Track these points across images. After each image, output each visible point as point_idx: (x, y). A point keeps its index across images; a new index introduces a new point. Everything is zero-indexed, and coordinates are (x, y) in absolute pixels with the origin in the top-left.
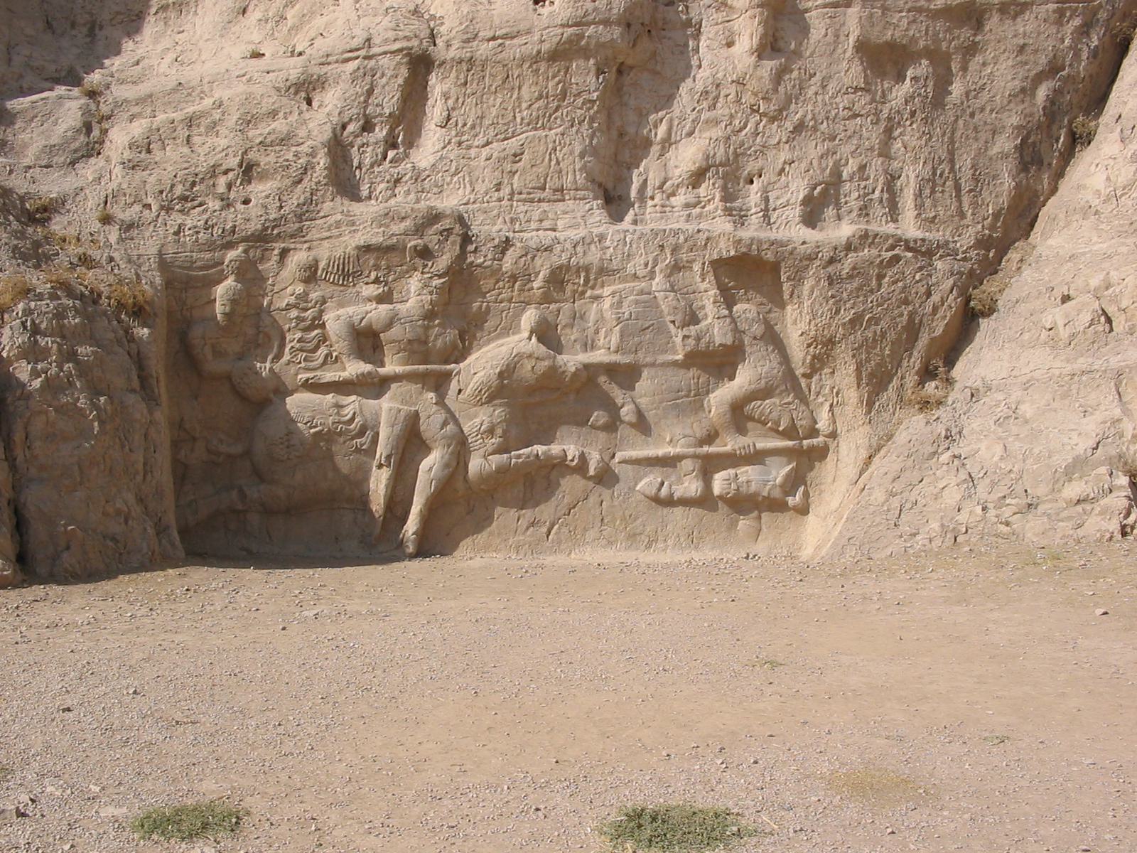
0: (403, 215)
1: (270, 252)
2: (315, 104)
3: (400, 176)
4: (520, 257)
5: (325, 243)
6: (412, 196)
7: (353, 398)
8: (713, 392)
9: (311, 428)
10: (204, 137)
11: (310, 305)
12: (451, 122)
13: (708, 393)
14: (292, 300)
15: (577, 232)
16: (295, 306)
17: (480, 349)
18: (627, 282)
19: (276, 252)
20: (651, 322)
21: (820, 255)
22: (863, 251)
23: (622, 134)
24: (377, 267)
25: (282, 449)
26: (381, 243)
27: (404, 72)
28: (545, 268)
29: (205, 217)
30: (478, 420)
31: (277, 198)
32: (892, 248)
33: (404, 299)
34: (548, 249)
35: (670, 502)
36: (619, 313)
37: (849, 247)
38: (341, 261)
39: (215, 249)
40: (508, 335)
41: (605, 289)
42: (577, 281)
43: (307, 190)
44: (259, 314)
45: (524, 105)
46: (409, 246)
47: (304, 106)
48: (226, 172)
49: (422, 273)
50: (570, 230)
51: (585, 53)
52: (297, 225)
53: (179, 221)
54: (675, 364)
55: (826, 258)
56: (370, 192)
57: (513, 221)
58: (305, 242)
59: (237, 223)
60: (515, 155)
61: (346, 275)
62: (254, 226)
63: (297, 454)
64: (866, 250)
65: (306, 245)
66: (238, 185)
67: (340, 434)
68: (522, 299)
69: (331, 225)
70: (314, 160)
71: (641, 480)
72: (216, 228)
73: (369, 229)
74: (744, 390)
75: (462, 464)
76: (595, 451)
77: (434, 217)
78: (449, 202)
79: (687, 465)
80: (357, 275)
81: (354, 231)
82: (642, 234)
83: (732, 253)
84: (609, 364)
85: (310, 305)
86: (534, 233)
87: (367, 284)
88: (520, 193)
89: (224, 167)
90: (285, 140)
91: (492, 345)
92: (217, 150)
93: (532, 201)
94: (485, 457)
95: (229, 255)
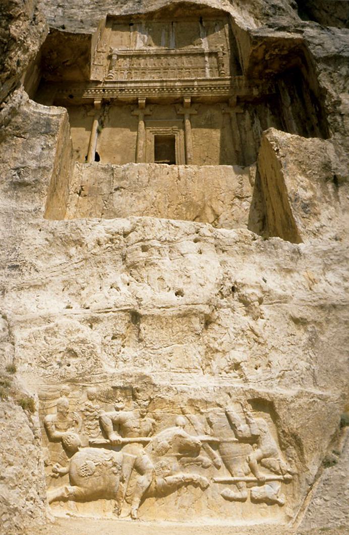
2: (93, 328)
5: (99, 384)
13: (248, 454)
14: (87, 408)
16: (87, 410)
27: (128, 318)
30: (161, 462)
32: (312, 397)
34: (185, 392)
35: (231, 500)
47: (90, 329)
48: (60, 352)
54: (236, 442)
55: (290, 401)
57: (172, 380)
60: (170, 353)
61: (108, 398)
62: (73, 376)
65: (92, 385)
67: (106, 466)
77: (142, 377)
78: (147, 371)
79: (241, 484)
81: (111, 380)
90: (83, 341)
94: (163, 478)
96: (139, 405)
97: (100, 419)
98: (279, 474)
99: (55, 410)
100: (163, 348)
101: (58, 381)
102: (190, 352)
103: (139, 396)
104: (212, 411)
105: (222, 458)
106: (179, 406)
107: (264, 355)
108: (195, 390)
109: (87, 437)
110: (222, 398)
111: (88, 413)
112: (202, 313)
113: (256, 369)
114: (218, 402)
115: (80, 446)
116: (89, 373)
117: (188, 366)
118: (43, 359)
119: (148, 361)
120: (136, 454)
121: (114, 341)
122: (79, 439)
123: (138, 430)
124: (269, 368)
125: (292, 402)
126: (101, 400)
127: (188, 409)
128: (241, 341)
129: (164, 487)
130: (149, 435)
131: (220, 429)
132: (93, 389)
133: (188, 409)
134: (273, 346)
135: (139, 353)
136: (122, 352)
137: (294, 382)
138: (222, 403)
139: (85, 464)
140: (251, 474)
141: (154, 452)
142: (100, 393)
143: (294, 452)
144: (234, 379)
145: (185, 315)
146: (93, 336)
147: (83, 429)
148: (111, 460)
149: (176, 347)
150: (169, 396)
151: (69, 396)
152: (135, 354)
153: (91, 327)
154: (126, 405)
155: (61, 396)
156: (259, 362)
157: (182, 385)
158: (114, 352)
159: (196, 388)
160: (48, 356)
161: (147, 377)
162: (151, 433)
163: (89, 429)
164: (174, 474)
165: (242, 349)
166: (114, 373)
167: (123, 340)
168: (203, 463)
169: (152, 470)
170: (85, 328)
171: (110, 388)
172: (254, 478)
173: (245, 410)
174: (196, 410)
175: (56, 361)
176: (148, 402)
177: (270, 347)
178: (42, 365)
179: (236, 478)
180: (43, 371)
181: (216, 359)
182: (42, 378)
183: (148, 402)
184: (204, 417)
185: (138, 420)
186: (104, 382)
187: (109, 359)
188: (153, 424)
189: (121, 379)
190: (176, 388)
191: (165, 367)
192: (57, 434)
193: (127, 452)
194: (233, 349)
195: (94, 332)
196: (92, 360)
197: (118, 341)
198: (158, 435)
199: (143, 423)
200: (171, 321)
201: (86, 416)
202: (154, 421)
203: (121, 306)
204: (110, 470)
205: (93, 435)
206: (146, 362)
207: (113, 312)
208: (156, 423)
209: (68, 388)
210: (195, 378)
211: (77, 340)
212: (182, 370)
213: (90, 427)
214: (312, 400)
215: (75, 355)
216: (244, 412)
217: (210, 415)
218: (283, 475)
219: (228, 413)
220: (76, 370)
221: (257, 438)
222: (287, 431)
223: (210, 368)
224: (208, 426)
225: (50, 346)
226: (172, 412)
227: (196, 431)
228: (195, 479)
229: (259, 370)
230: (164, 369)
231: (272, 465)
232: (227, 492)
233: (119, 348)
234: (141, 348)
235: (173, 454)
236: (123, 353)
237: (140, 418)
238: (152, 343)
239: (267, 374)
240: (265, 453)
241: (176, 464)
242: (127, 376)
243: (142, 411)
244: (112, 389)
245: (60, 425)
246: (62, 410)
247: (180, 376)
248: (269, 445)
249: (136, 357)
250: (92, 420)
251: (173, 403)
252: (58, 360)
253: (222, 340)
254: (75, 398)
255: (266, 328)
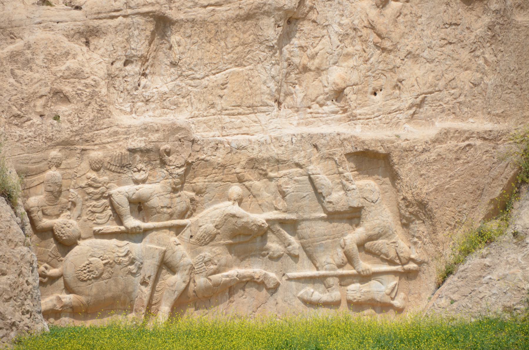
0: (156, 128)
1: (74, 151)
2: (92, 47)
3: (150, 98)
4: (227, 154)
5: (108, 146)
6: (158, 112)
7: (126, 242)
8: (345, 236)
9: (102, 260)
10: (22, 71)
11: (100, 185)
12: (182, 61)
13: (343, 235)
14: (90, 182)
15: (262, 135)
16: (90, 186)
17: (202, 211)
18: (292, 168)
19: (79, 151)
20: (307, 193)
21: (416, 147)
22: (446, 143)
23: (290, 65)
24: (141, 161)
25: (85, 273)
26: (144, 147)
27: (151, 27)
28: (243, 160)
29: (33, 129)
30: (202, 254)
31: (76, 115)
32: (468, 138)
33: (157, 181)
34: (244, 148)
36: (287, 188)
37: (436, 141)
38: (120, 158)
39: (41, 151)
40: (219, 203)
41: (280, 172)
42: (262, 167)
43: (94, 110)
44: (68, 190)
45: (229, 50)
46: (161, 149)
47: (85, 48)
48: (41, 97)
49: (169, 165)
50: (257, 134)
51: (268, 14)
52: (91, 134)
53: (18, 133)
54: (322, 219)
55: (420, 150)
56: (131, 108)
57: (223, 128)
58: (96, 145)
59: (53, 134)
60: (223, 85)
61: (122, 166)
62: (65, 135)
63: (94, 276)
64: (448, 142)
65: (96, 147)
66: (49, 106)
67: (120, 263)
68: (228, 180)
69: (111, 134)
70: (97, 90)
71: (300, 291)
72: (41, 136)
73: (135, 138)
74: (364, 234)
75: (192, 280)
76: (272, 272)
77: (175, 129)
79: (331, 281)
80: (128, 166)
81: (126, 139)
82: (302, 137)
83: (358, 150)
84: (280, 219)
85: (100, 185)
86: (235, 137)
87: (135, 172)
88: (226, 110)
89: (38, 95)
90: (77, 75)
91: (211, 208)
92: (33, 82)
93: (233, 115)
94: (207, 276)
95: (51, 154)
96: (171, 174)
97: (110, 196)
98: (395, 264)
99: (42, 188)
100: (212, 77)
101: (44, 146)
102: (256, 79)
103: (170, 161)
104: (285, 175)
105: (301, 244)
106: (233, 171)
107: (391, 70)
108: (261, 144)
109: (91, 223)
110: (303, 154)
111: (91, 190)
112: (279, 9)
113: (375, 94)
114: (297, 161)
115: (79, 238)
116: (90, 128)
117: (251, 102)
118: (15, 110)
119: (185, 100)
120: (164, 245)
121: (128, 68)
122: (78, 228)
123: (169, 211)
124: (398, 91)
125: (424, 151)
126: (111, 170)
127: (247, 175)
128: (350, 49)
129: (207, 289)
130: (187, 215)
131: (297, 202)
132: (96, 154)
133: (247, 175)
134: (410, 53)
135: (171, 85)
136: (142, 85)
137: (443, 111)
138: (303, 162)
139: (87, 262)
140: (348, 265)
141: (193, 240)
142: (108, 159)
143: (422, 228)
144: (333, 116)
145: (248, 17)
146: (93, 63)
147: (84, 212)
148: (126, 255)
149: (233, 73)
150: (219, 157)
151: (62, 166)
152: (165, 89)
153: (87, 43)
154: (150, 175)
155: (50, 168)
156: (382, 81)
157: (240, 137)
158: (129, 87)
159: (262, 140)
160: (22, 105)
161: (183, 129)
162: (189, 213)
163: (94, 212)
164: (224, 271)
165: (352, 62)
166: (130, 127)
167: (143, 65)
168: (271, 253)
169: (189, 267)
170: (78, 47)
171: (124, 151)
172: (353, 271)
173: (341, 169)
174: (261, 174)
175: (36, 112)
176: (183, 169)
177: (402, 54)
178: (15, 122)
179: (322, 272)
180: (18, 131)
181: (304, 84)
182: (18, 144)
183: (183, 169)
184: (273, 183)
185: (168, 195)
186: (116, 142)
187: (121, 100)
188: (192, 200)
189: (142, 136)
190: (229, 143)
191: (213, 107)
192: (46, 222)
193: (151, 242)
194: (335, 64)
195: (95, 56)
196: (94, 106)
197: (134, 68)
198: (200, 215)
199: (178, 200)
200: (223, 28)
201: (88, 194)
202: (193, 194)
203: (138, 6)
204: (126, 269)
205: (99, 221)
206: (181, 100)
207: (125, 16)
208: (197, 198)
209: (60, 154)
210: (263, 123)
211: (67, 73)
212: (241, 110)
213: (94, 209)
214: (467, 143)
215: (66, 99)
216: (340, 173)
217: (282, 181)
218: (403, 264)
219: (312, 176)
220: (69, 125)
221: (360, 211)
222: (409, 198)
223: (293, 98)
224: (279, 197)
225: (25, 87)
226: (221, 180)
227: (260, 205)
228: (256, 277)
229: (380, 95)
230: (213, 111)
231: (384, 251)
232: (307, 293)
233: (136, 80)
234: (173, 77)
235: (222, 242)
236: (145, 87)
237: (171, 192)
238: (191, 69)
239: (393, 101)
240: (372, 233)
241: (226, 257)
242: (150, 131)
243: (174, 183)
244: (128, 153)
245: (50, 210)
246: (51, 189)
247: (237, 120)
248: (378, 222)
249: (165, 93)
250: (97, 199)
251: (224, 166)
252: (39, 109)
253: (316, 49)
254: (70, 168)
255: (401, 19)
